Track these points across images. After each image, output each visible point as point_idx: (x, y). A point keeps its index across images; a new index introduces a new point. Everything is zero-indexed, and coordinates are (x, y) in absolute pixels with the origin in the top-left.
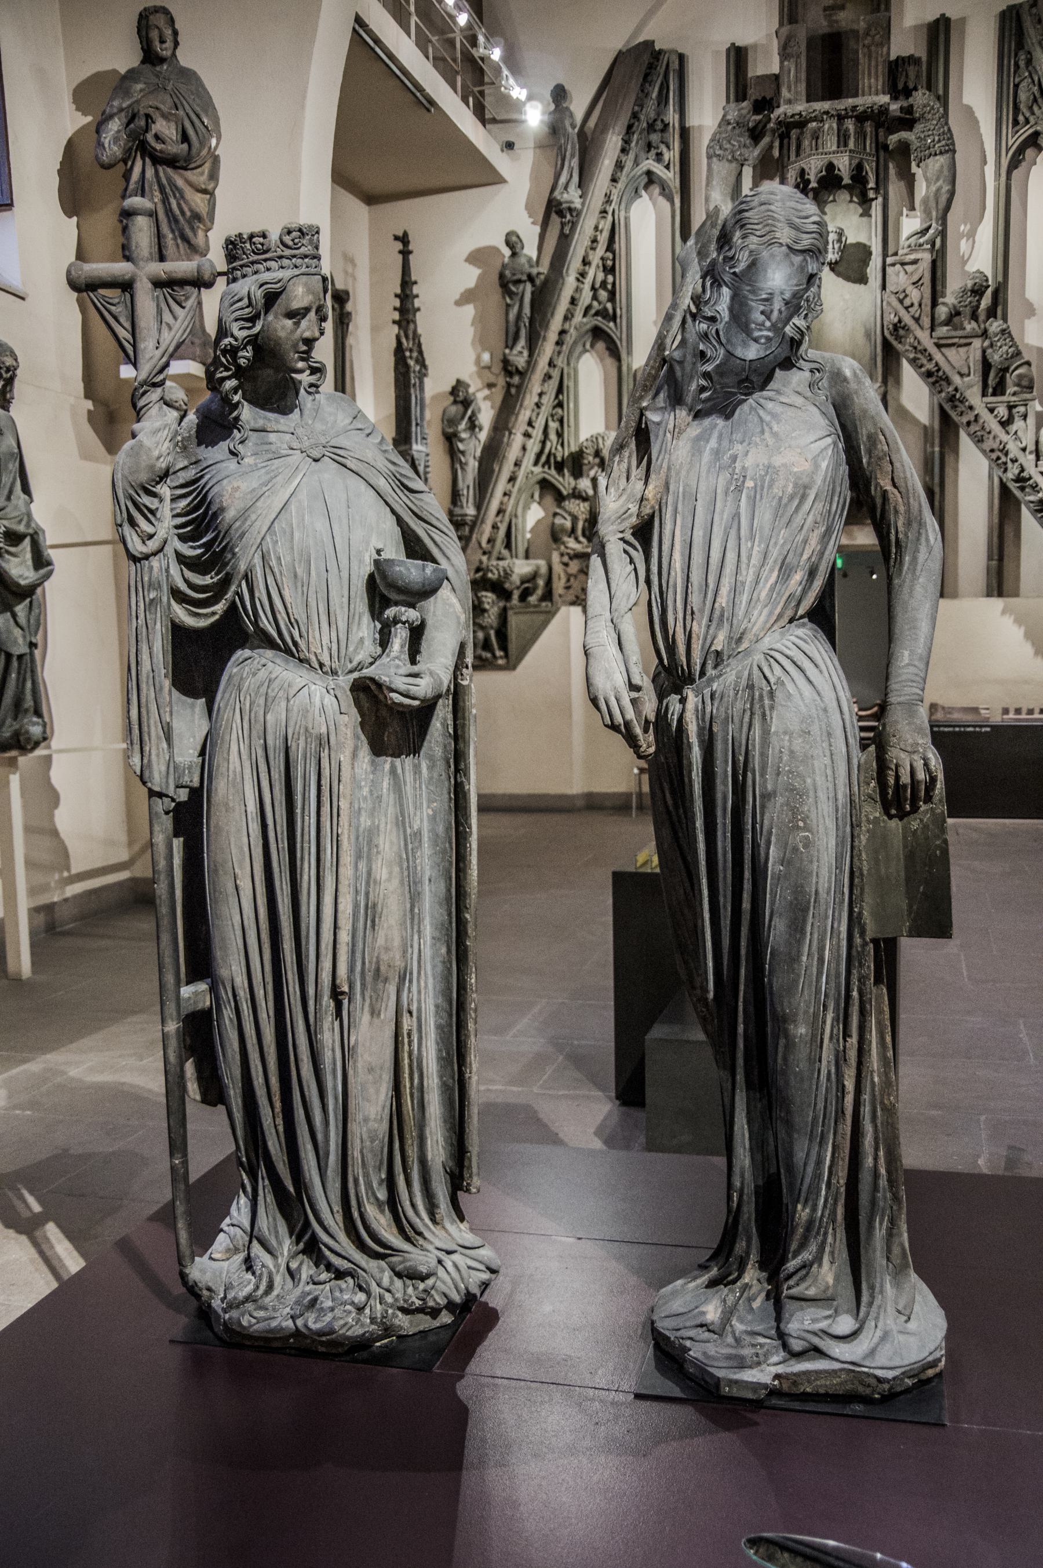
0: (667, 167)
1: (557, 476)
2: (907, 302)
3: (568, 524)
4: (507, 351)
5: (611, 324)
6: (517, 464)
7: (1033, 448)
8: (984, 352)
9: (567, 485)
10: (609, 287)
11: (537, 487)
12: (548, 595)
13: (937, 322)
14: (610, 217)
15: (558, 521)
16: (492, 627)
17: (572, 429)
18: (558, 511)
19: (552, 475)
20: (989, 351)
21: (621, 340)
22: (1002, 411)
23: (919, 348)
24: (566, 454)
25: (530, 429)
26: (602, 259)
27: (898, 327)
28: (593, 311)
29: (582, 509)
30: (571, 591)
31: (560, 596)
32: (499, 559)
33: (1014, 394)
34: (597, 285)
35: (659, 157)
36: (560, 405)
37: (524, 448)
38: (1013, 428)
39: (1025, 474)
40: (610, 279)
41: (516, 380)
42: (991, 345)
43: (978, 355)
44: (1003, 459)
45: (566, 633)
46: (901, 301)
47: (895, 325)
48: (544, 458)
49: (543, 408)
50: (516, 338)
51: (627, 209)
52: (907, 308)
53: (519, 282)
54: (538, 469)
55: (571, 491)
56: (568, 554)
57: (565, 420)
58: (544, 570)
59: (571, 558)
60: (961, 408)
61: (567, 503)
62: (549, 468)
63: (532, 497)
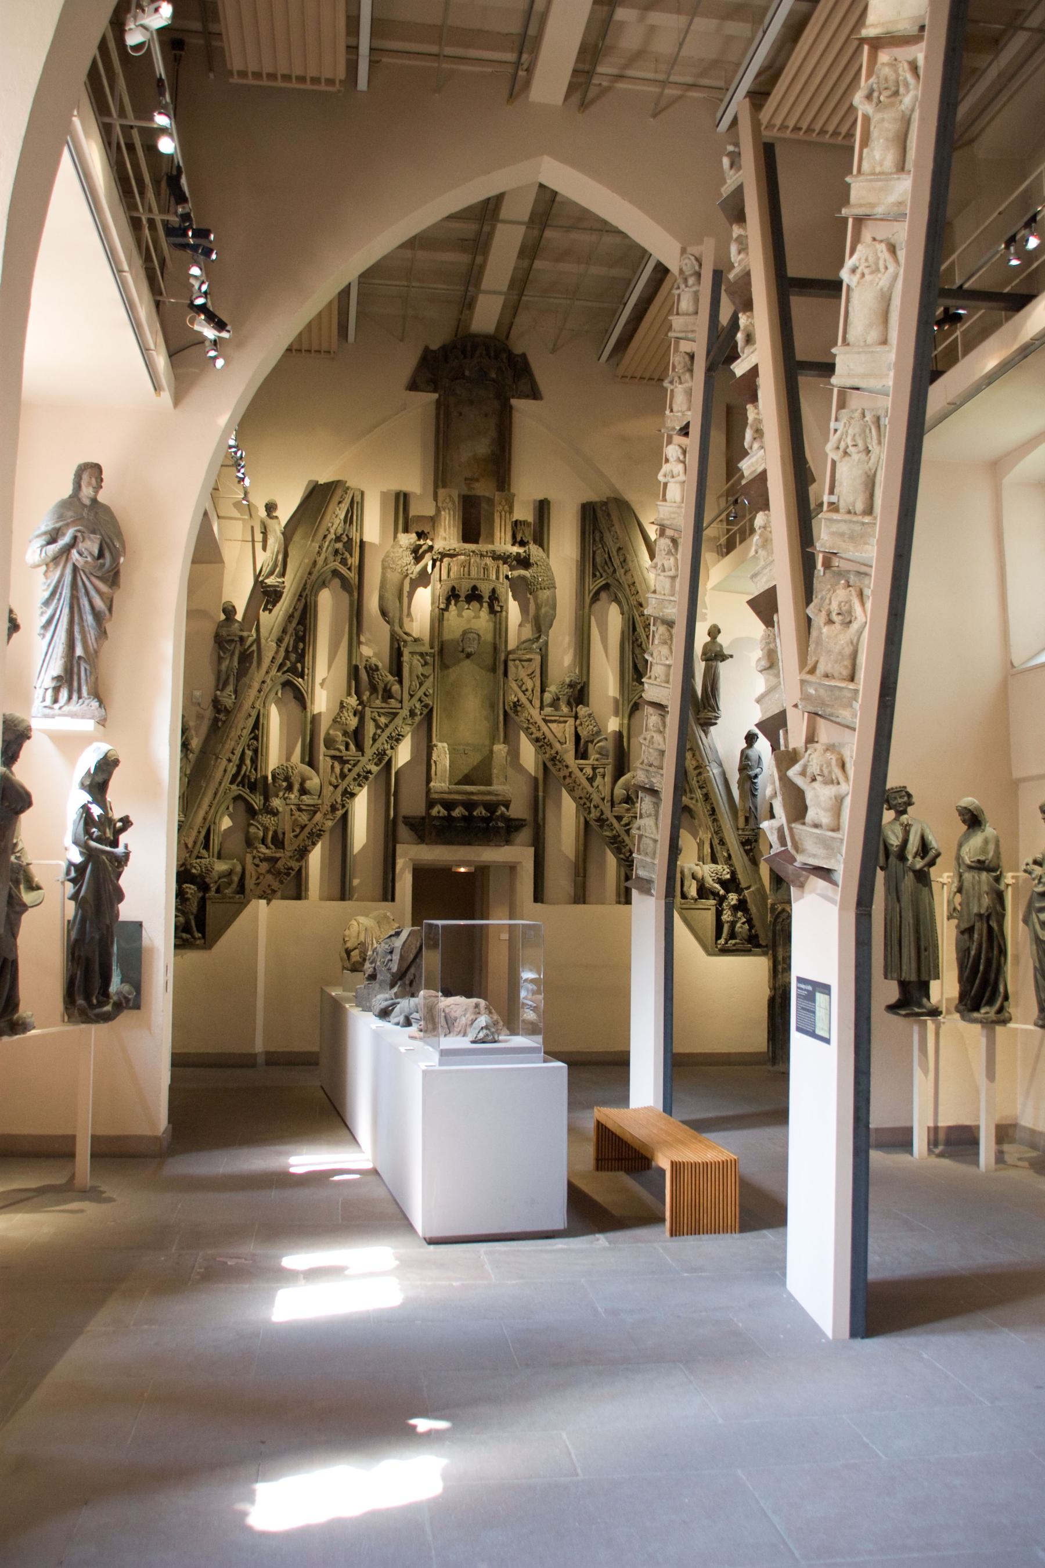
0: (349, 569)
2: (524, 688)
3: (261, 834)
4: (218, 693)
5: (300, 680)
6: (220, 783)
7: (610, 799)
8: (576, 728)
9: (258, 801)
10: (300, 651)
12: (241, 888)
13: (545, 703)
14: (303, 600)
15: (252, 830)
16: (192, 914)
19: (245, 793)
20: (579, 728)
21: (307, 693)
22: (589, 771)
23: (531, 721)
24: (259, 776)
26: (295, 629)
27: (517, 705)
28: (285, 669)
32: (198, 857)
33: (597, 760)
34: (290, 649)
35: (344, 562)
36: (256, 738)
37: (225, 771)
38: (595, 784)
39: (604, 817)
40: (301, 645)
41: (222, 717)
42: (581, 724)
43: (573, 728)
44: (588, 804)
45: (256, 920)
46: (520, 687)
47: (514, 703)
48: (239, 779)
50: (226, 683)
51: (316, 595)
52: (523, 692)
53: (233, 641)
54: (234, 787)
55: (262, 807)
56: (259, 857)
57: (260, 750)
58: (239, 868)
59: (261, 861)
60: (559, 766)
62: (243, 786)
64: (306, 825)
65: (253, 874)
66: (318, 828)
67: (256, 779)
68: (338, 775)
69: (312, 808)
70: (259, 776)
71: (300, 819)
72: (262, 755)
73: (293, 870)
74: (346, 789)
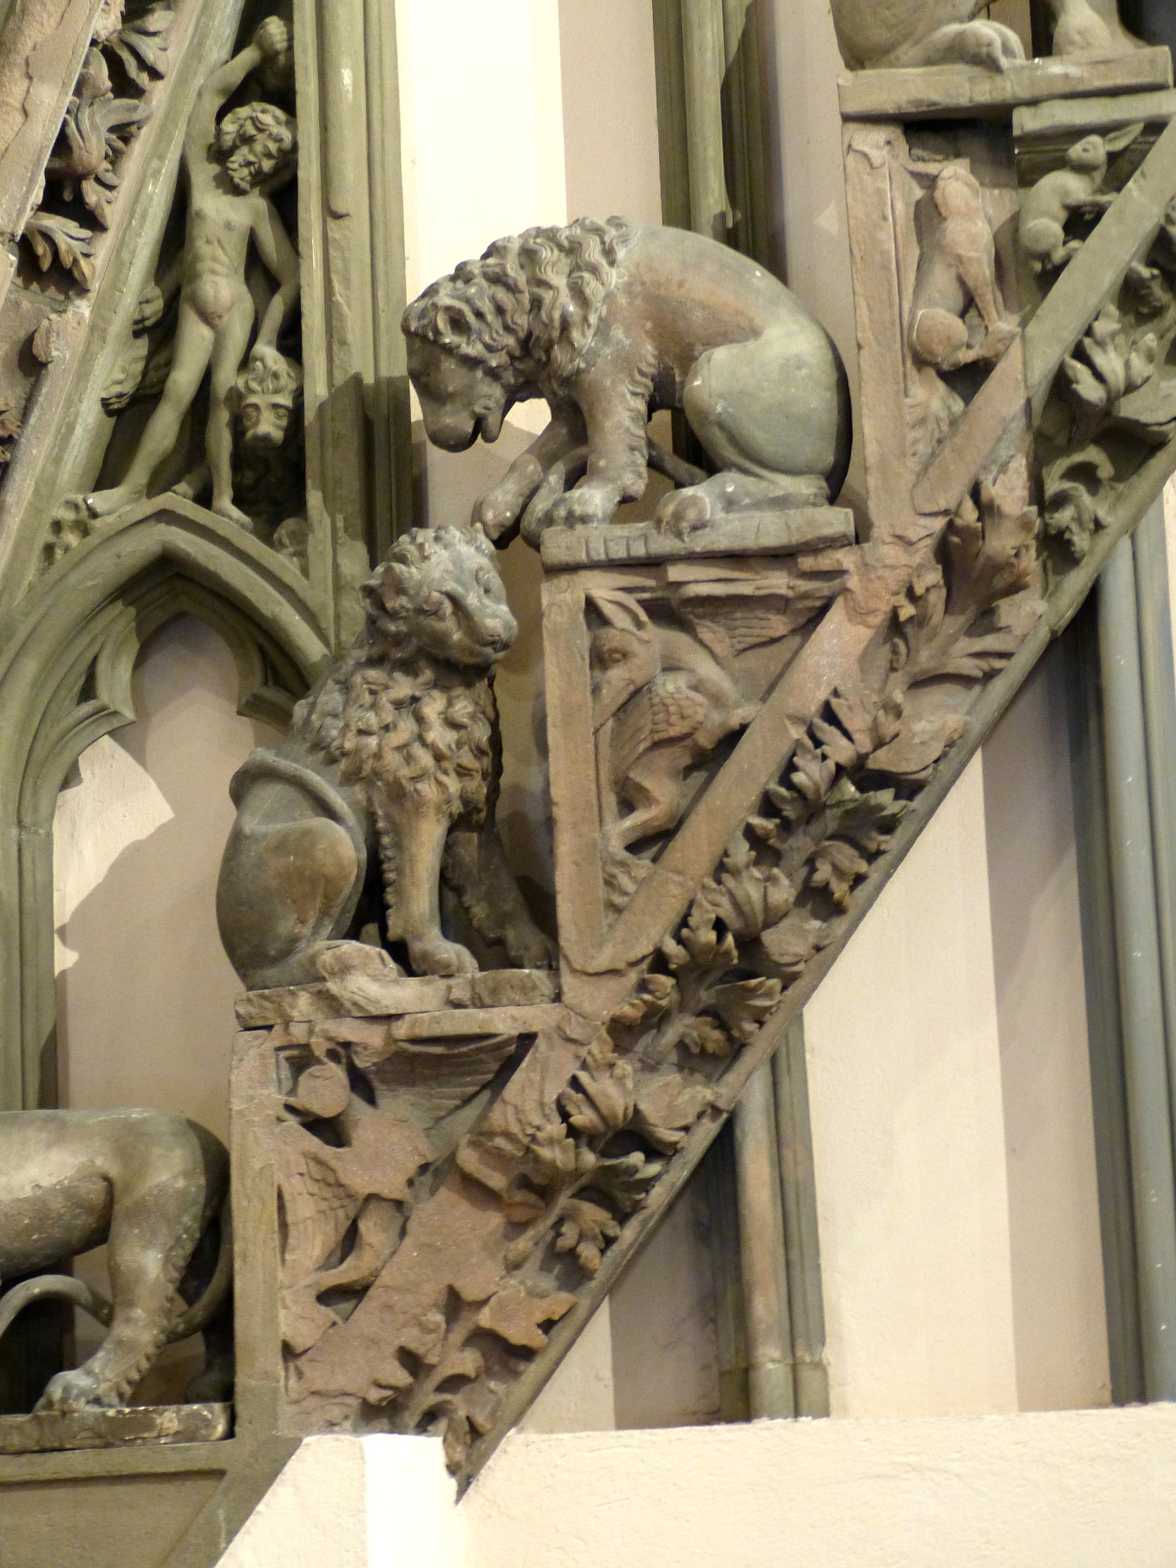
1: (253, 545)
9: (319, 594)
11: (122, 618)
17: (355, 232)
18: (269, 757)
24: (317, 390)
25: (62, 228)
29: (440, 735)
30: (367, 1315)
31: (288, 1352)
49: (158, 94)
56: (342, 1052)
61: (330, 697)
62: (204, 498)
63: (88, 692)
64: (732, 738)
65: (302, 1209)
66: (840, 750)
67: (296, 413)
68: (982, 271)
69: (777, 582)
70: (317, 390)
71: (671, 686)
72: (331, 214)
73: (655, 1150)
74: (1061, 383)
